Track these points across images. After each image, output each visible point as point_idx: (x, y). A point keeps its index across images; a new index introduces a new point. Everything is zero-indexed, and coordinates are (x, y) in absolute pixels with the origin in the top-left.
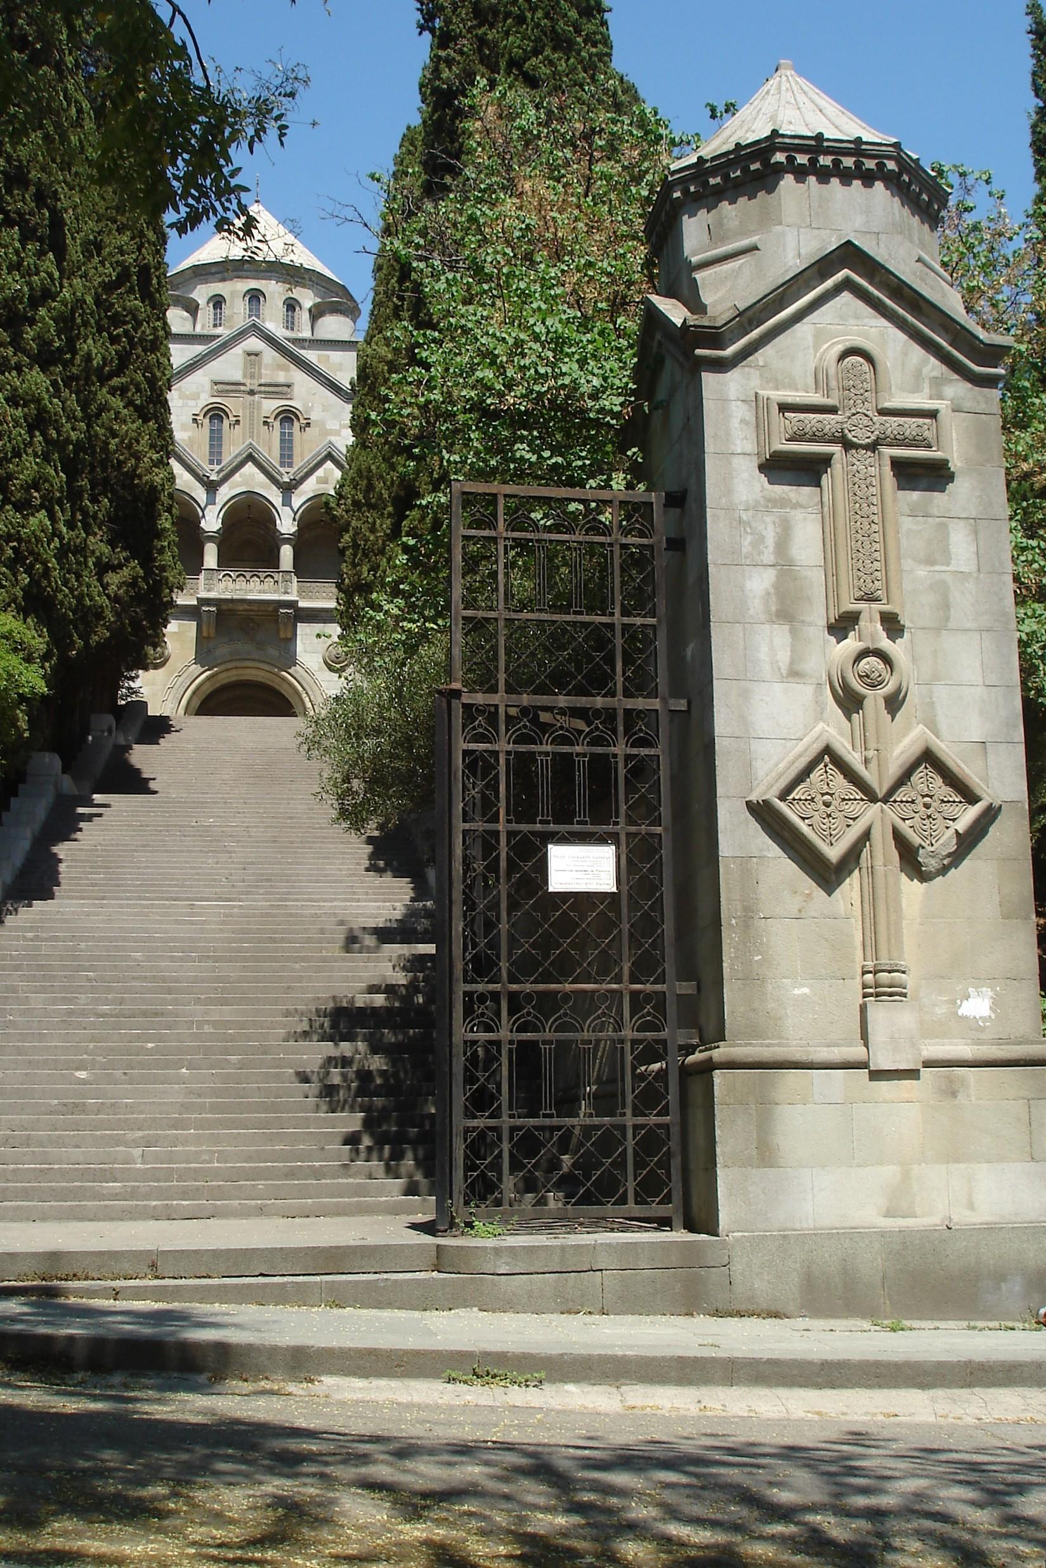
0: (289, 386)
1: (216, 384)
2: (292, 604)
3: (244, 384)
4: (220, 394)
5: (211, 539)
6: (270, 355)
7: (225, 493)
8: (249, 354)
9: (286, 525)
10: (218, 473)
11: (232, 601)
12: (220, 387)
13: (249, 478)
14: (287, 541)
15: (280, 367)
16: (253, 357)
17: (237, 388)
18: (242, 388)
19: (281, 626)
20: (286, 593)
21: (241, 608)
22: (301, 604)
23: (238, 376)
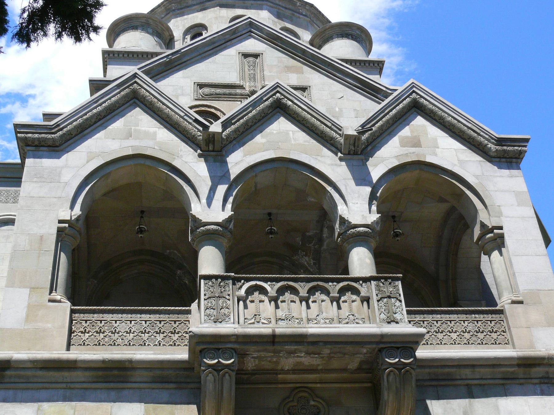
0: (303, 89)
1: (201, 86)
2: (407, 345)
3: (241, 87)
4: (205, 97)
5: (211, 236)
6: (272, 57)
7: (238, 161)
8: (246, 55)
9: (356, 208)
10: (225, 125)
11: (273, 340)
12: (207, 90)
13: (281, 139)
14: (360, 239)
15: (288, 69)
16: (251, 59)
17: (233, 91)
18: (238, 91)
19: (388, 396)
20: (391, 321)
21: (288, 363)
22: (422, 353)
23: (232, 78)
